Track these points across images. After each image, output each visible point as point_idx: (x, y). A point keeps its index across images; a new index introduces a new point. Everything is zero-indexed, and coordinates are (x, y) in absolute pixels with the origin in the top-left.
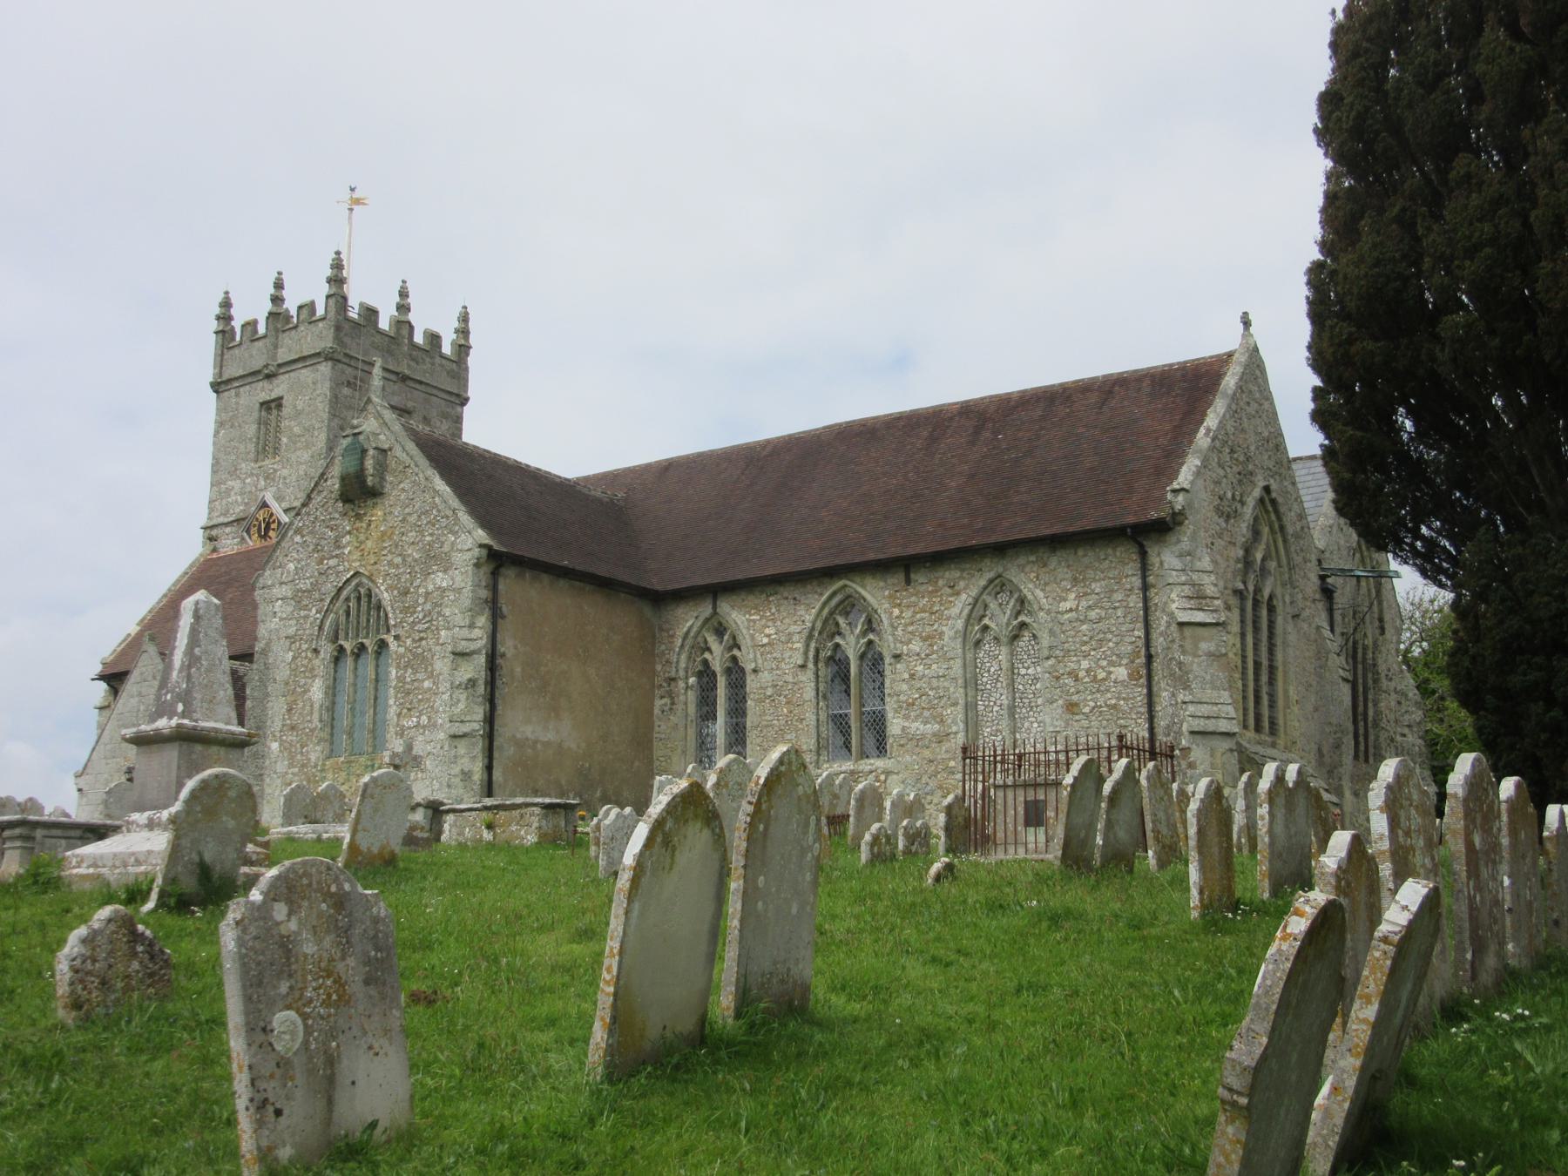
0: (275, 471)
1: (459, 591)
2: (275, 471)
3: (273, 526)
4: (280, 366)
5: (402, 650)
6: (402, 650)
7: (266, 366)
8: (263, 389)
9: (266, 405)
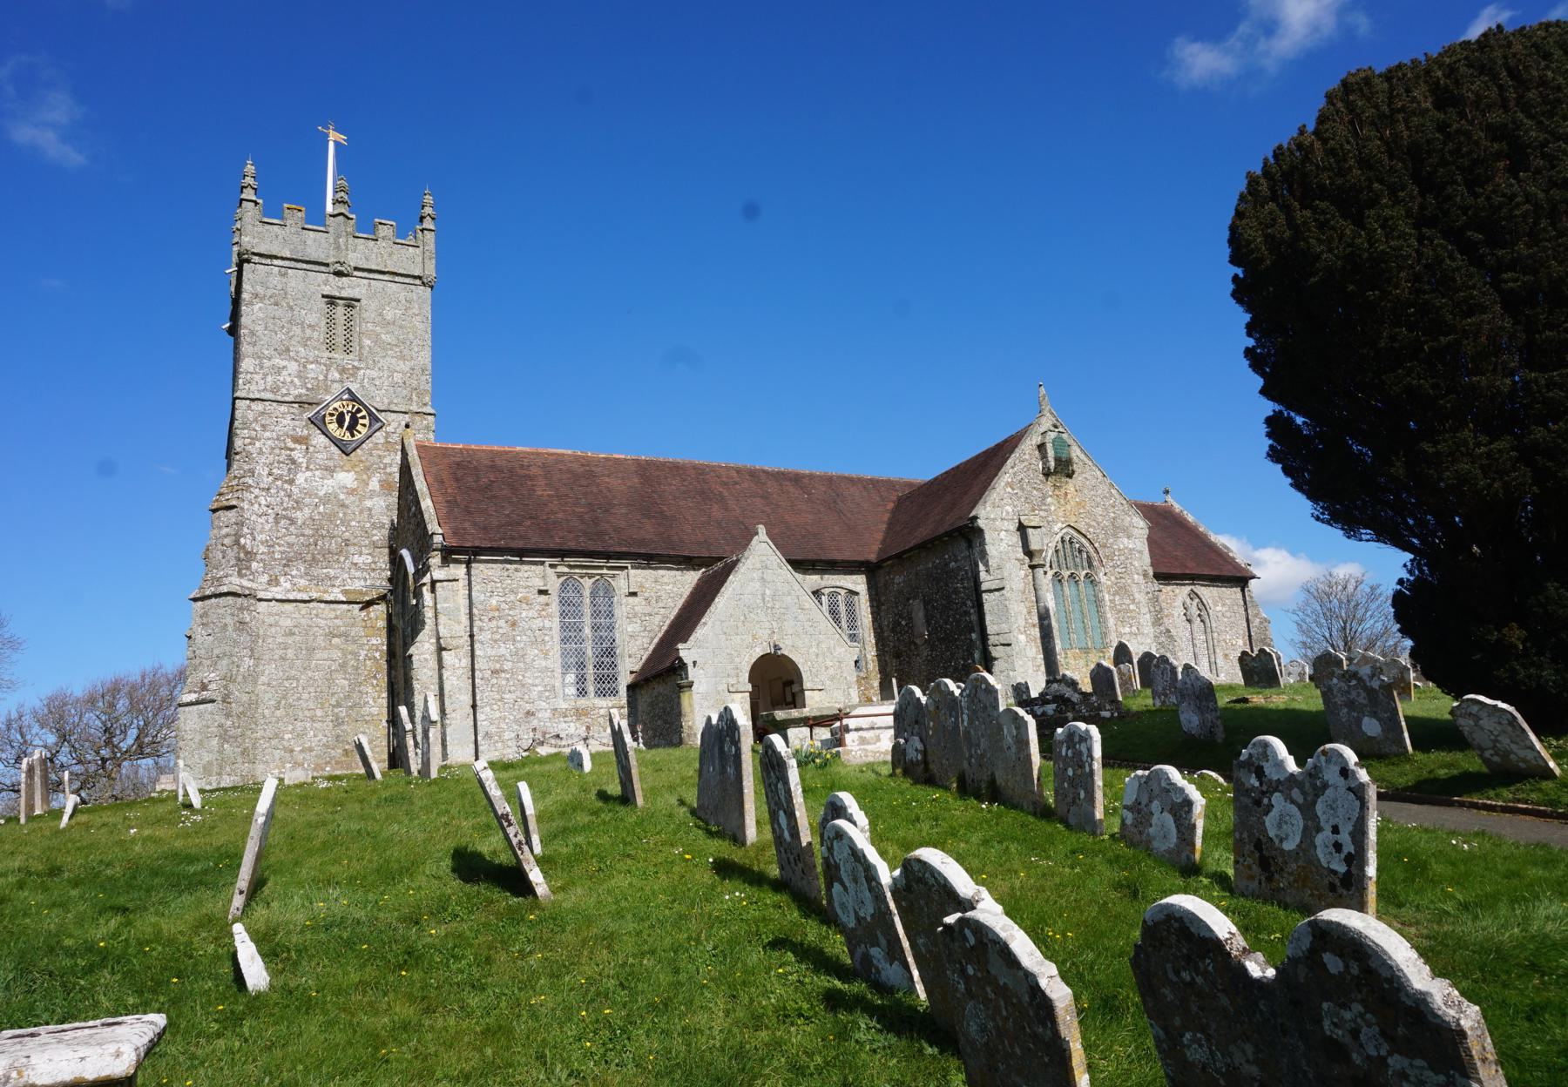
0: (358, 369)
1: (1140, 552)
2: (358, 369)
3: (361, 421)
4: (356, 269)
5: (1109, 583)
6: (1109, 583)
7: (342, 264)
8: (326, 283)
9: (331, 300)
